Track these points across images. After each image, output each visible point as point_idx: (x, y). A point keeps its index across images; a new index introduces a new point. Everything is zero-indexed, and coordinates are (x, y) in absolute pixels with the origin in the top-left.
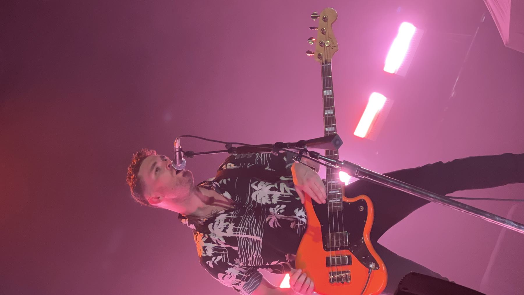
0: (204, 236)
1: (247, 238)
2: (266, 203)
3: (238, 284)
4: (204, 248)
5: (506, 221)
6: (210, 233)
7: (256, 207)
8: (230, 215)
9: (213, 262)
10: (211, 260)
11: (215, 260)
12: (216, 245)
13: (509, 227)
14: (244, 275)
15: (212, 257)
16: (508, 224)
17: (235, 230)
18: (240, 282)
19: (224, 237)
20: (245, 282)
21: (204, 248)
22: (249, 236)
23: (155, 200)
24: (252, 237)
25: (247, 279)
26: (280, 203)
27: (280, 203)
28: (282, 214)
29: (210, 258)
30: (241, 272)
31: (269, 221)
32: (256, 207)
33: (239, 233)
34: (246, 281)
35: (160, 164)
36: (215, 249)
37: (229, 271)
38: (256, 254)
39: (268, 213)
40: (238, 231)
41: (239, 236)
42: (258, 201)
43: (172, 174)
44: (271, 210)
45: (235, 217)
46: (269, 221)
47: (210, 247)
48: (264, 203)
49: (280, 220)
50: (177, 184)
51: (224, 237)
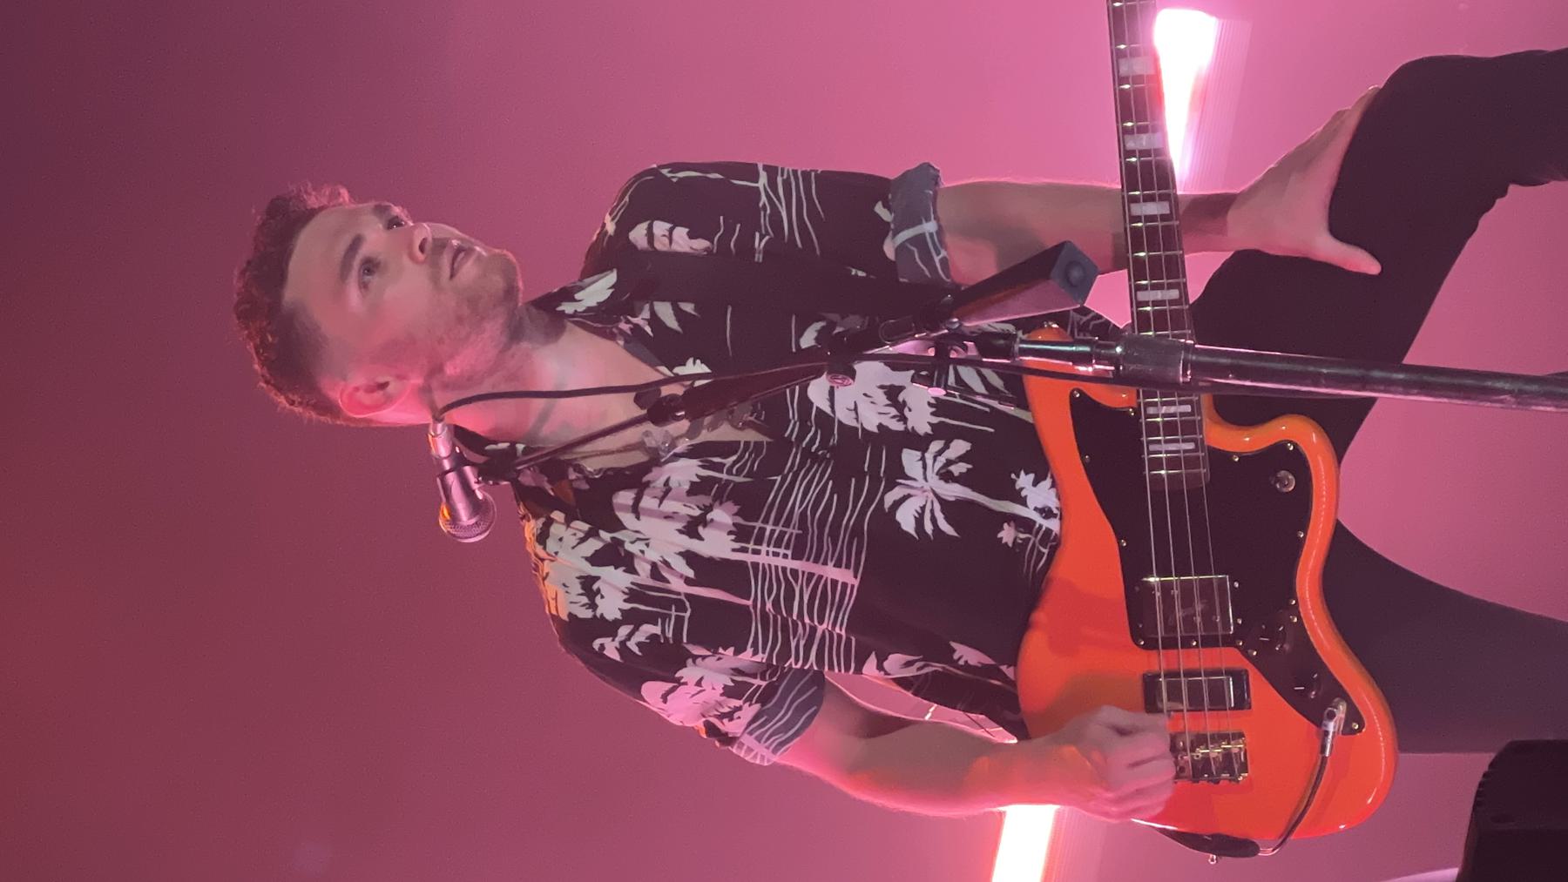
1: (794, 572)
2: (880, 426)
4: (588, 583)
6: (620, 526)
7: (834, 440)
8: (718, 467)
9: (623, 643)
10: (614, 635)
12: (644, 575)
14: (757, 682)
18: (740, 708)
19: (690, 557)
20: (757, 707)
21: (588, 583)
23: (361, 395)
24: (817, 569)
26: (942, 433)
27: (939, 432)
28: (961, 480)
29: (610, 628)
30: (737, 671)
31: (897, 504)
32: (834, 440)
33: (764, 548)
34: (763, 700)
35: (375, 238)
36: (634, 594)
37: (688, 673)
38: (834, 626)
39: (897, 473)
40: (759, 542)
41: (762, 559)
42: (843, 416)
43: (435, 279)
44: (910, 458)
46: (897, 504)
47: (614, 586)
49: (952, 509)
50: (460, 320)
51: (690, 557)
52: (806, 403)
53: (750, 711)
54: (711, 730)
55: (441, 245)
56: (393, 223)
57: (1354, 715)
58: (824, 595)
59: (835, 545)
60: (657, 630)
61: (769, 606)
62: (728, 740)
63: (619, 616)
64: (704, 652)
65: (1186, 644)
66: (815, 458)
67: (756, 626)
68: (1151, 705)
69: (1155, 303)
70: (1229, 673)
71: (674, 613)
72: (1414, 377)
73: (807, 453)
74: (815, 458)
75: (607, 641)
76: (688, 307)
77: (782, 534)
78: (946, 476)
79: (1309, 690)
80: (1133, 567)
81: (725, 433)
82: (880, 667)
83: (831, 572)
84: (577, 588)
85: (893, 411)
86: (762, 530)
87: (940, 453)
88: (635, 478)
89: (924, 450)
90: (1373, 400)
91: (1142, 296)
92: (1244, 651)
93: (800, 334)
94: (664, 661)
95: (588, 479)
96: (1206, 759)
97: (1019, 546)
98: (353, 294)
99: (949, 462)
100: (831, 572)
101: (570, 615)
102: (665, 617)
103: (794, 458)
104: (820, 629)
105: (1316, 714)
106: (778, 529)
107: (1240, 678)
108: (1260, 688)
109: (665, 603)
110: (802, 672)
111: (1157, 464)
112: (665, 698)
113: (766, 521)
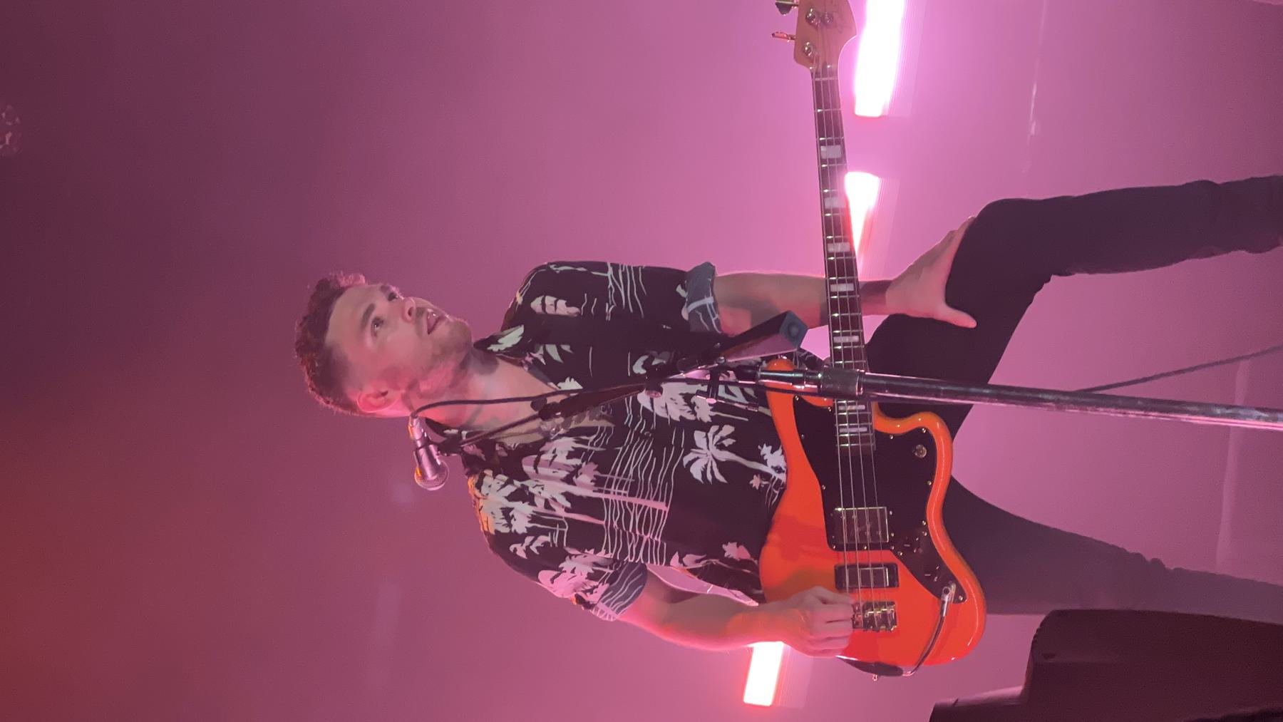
0: (509, 482)
1: (630, 505)
2: (681, 417)
3: (591, 591)
4: (507, 512)
6: (525, 477)
7: (654, 426)
8: (585, 442)
9: (528, 547)
10: (522, 542)
11: (531, 543)
14: (608, 571)
15: (523, 537)
17: (599, 483)
19: (568, 496)
20: (607, 586)
21: (507, 512)
22: (636, 501)
23: (373, 401)
24: (644, 502)
25: (611, 580)
26: (717, 421)
27: (717, 421)
28: (730, 449)
29: (519, 538)
30: (596, 564)
32: (654, 426)
34: (611, 580)
35: (382, 307)
36: (535, 518)
37: (567, 565)
39: (691, 445)
40: (609, 486)
42: (659, 411)
43: (419, 333)
44: (699, 436)
45: (598, 449)
47: (522, 512)
48: (676, 418)
49: (722, 466)
51: (568, 496)
52: (636, 404)
53: (603, 588)
54: (579, 599)
55: (421, 311)
56: (392, 297)
57: (960, 591)
58: (647, 520)
59: (654, 487)
60: (548, 539)
61: (615, 524)
62: (589, 606)
63: (525, 531)
64: (577, 552)
65: (860, 548)
66: (643, 437)
67: (607, 537)
68: (839, 585)
69: (844, 344)
70: (888, 566)
71: (558, 529)
72: (995, 392)
73: (637, 433)
74: (643, 437)
75: (518, 546)
76: (566, 348)
77: (623, 482)
78: (720, 447)
79: (933, 576)
80: (829, 502)
81: (586, 422)
82: (681, 561)
83: (651, 504)
84: (500, 515)
85: (688, 409)
86: (611, 480)
87: (717, 432)
88: (535, 449)
89: (707, 431)
90: (971, 406)
91: (837, 340)
92: (895, 553)
93: (633, 364)
94: (552, 558)
95: (508, 451)
96: (872, 616)
97: (762, 490)
98: (369, 341)
99: (722, 439)
100: (651, 504)
101: (496, 531)
102: (553, 531)
103: (630, 437)
104: (645, 538)
105: (938, 592)
106: (621, 478)
107: (892, 569)
108: (903, 573)
109: (553, 523)
110: (634, 564)
111: (844, 440)
112: (552, 581)
113: (613, 473)
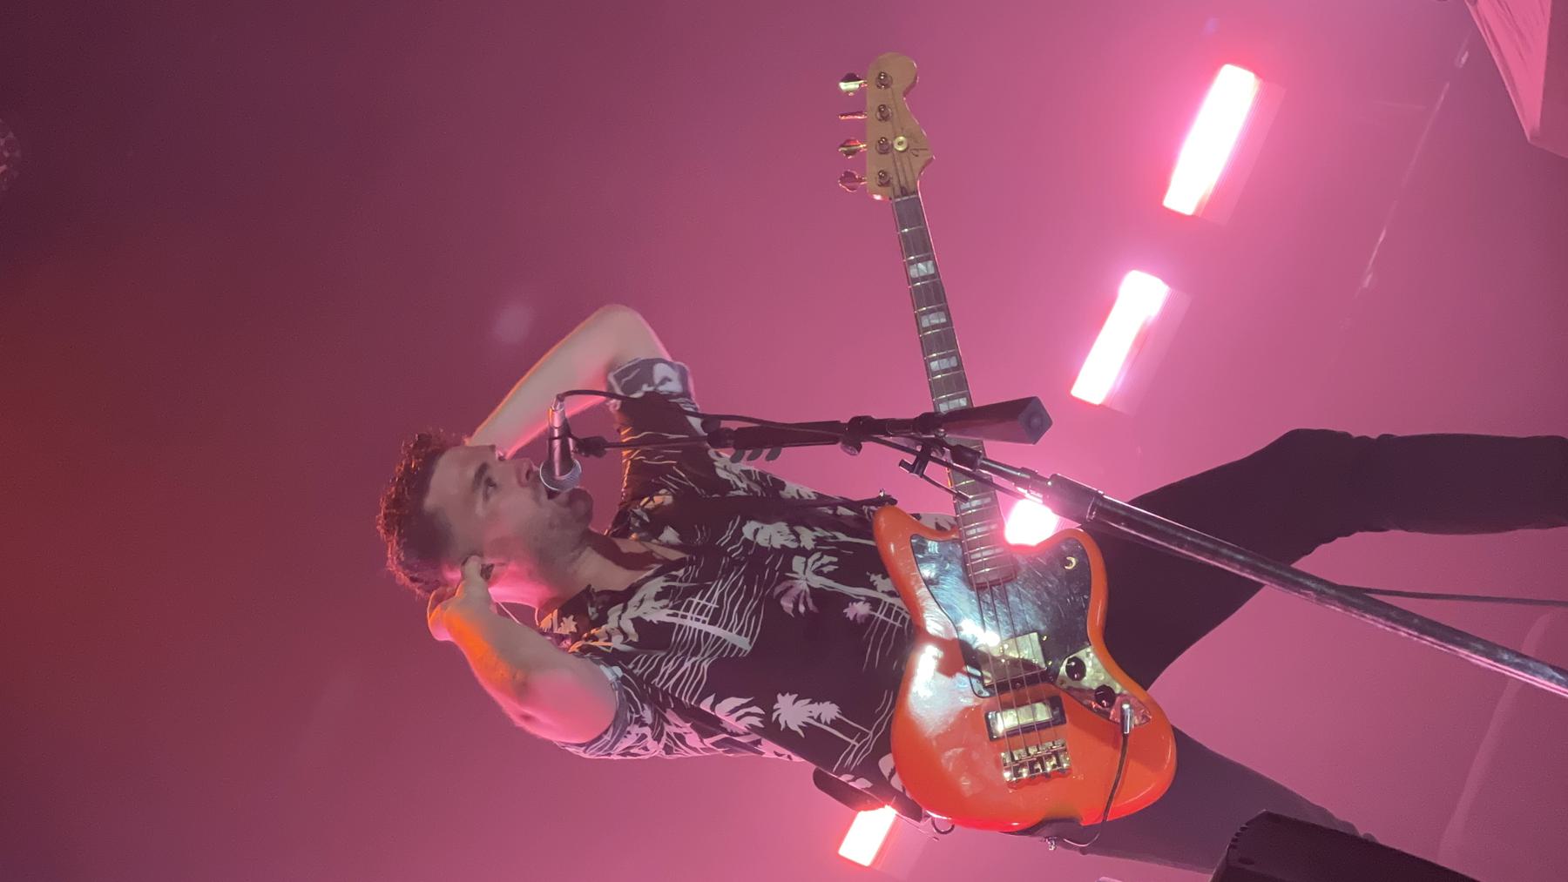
1: (707, 634)
5: (1531, 665)
13: (1540, 682)
16: (1535, 672)
22: (715, 631)
33: (689, 614)
40: (687, 610)
77: (705, 606)
100: (731, 637)
